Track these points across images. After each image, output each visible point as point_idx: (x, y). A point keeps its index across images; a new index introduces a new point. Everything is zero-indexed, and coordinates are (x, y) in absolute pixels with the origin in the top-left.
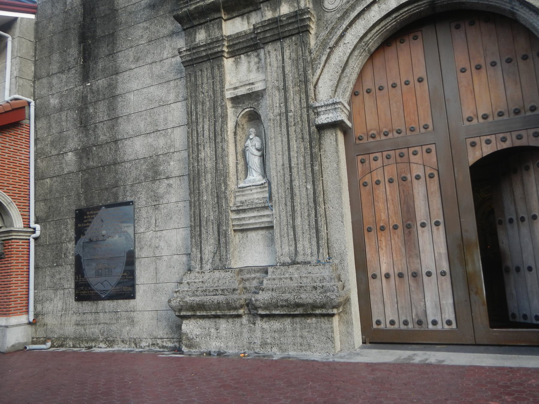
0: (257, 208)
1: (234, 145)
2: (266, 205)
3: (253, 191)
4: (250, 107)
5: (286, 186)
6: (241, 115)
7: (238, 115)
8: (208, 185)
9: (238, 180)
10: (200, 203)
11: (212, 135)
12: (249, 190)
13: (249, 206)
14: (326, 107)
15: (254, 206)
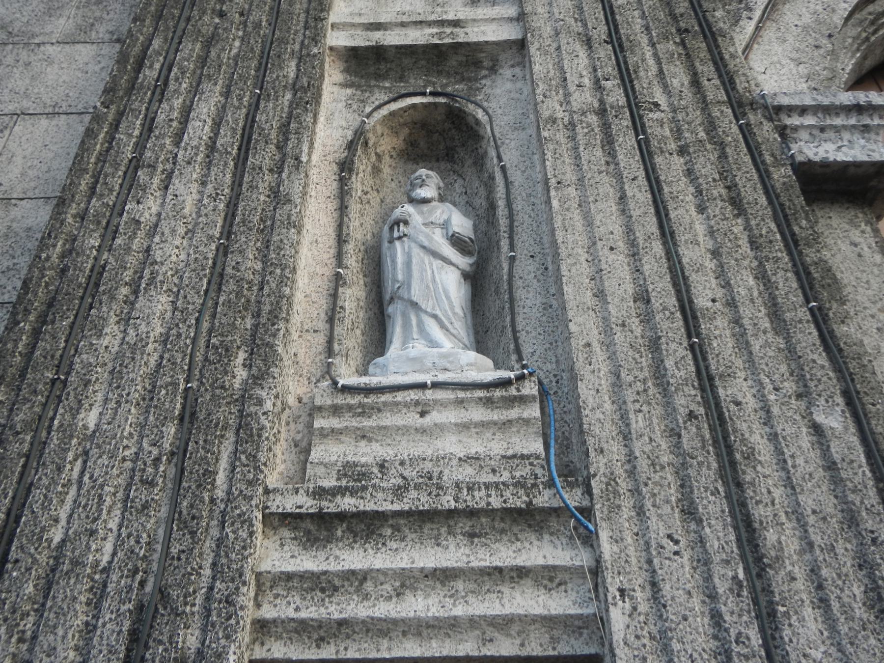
0: (472, 513)
1: (333, 205)
2: (544, 499)
3: (435, 417)
4: (433, 94)
5: (680, 401)
6: (384, 111)
7: (368, 109)
8: (137, 347)
9: (330, 351)
10: (39, 447)
11: (228, 139)
12: (407, 405)
13: (413, 494)
14: (820, 115)
15: (448, 502)
